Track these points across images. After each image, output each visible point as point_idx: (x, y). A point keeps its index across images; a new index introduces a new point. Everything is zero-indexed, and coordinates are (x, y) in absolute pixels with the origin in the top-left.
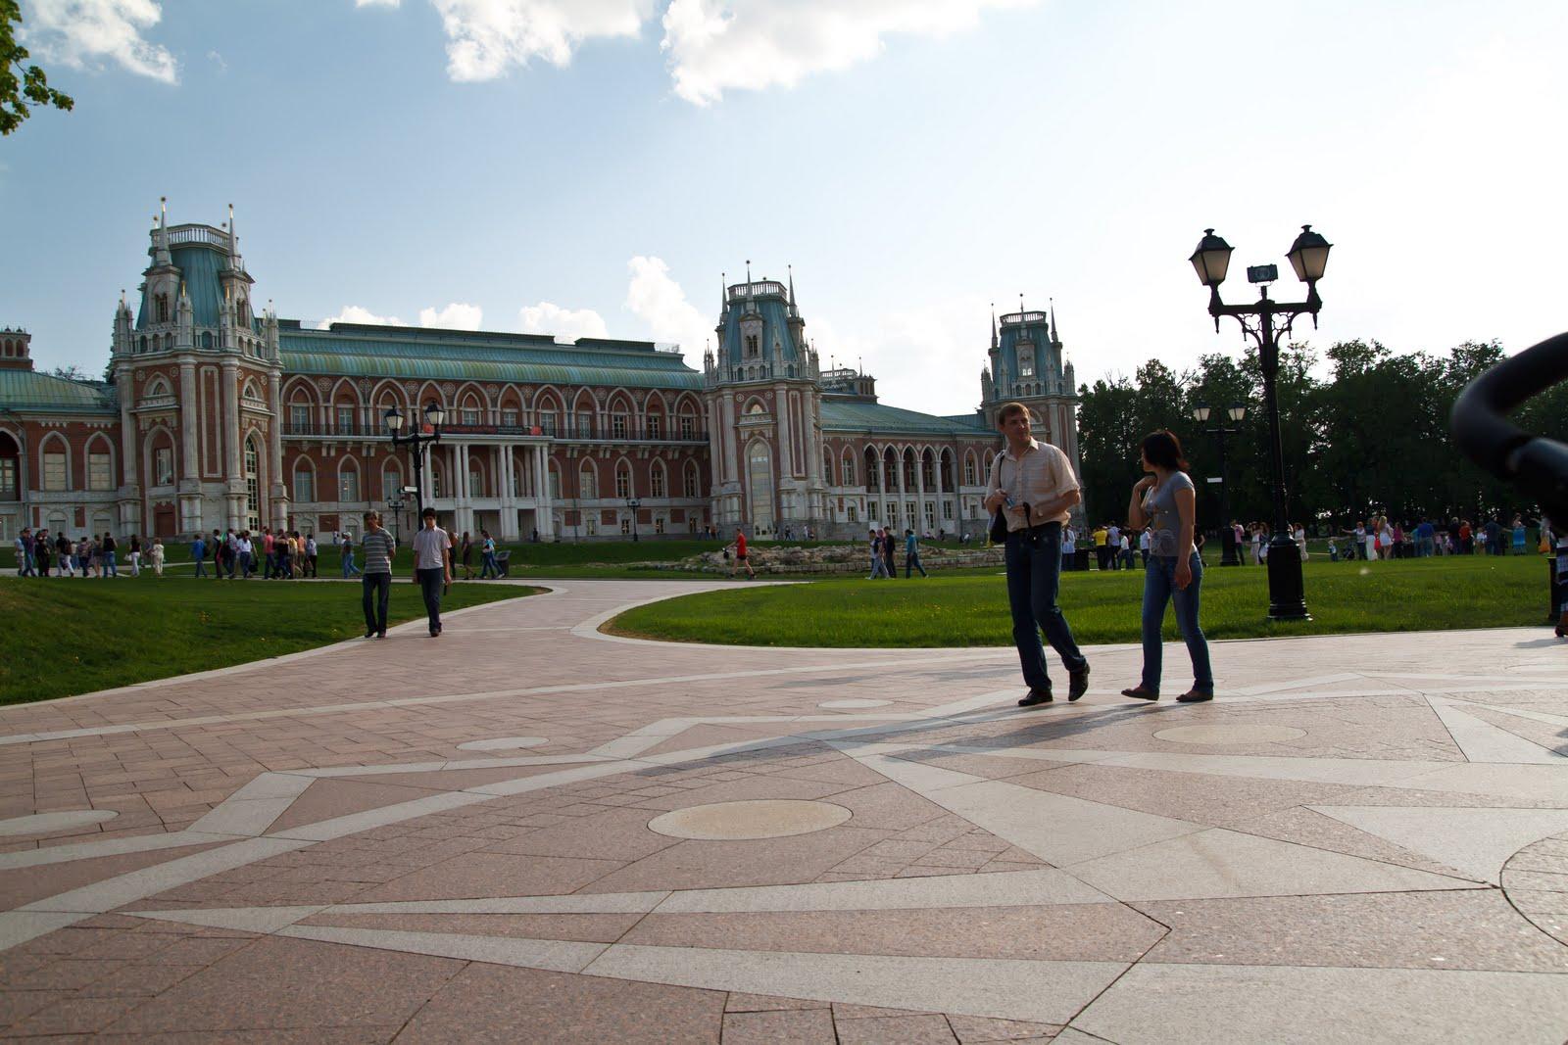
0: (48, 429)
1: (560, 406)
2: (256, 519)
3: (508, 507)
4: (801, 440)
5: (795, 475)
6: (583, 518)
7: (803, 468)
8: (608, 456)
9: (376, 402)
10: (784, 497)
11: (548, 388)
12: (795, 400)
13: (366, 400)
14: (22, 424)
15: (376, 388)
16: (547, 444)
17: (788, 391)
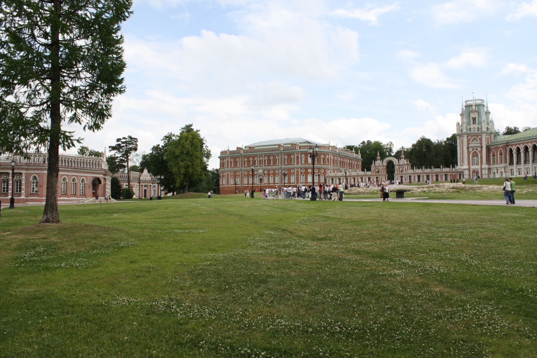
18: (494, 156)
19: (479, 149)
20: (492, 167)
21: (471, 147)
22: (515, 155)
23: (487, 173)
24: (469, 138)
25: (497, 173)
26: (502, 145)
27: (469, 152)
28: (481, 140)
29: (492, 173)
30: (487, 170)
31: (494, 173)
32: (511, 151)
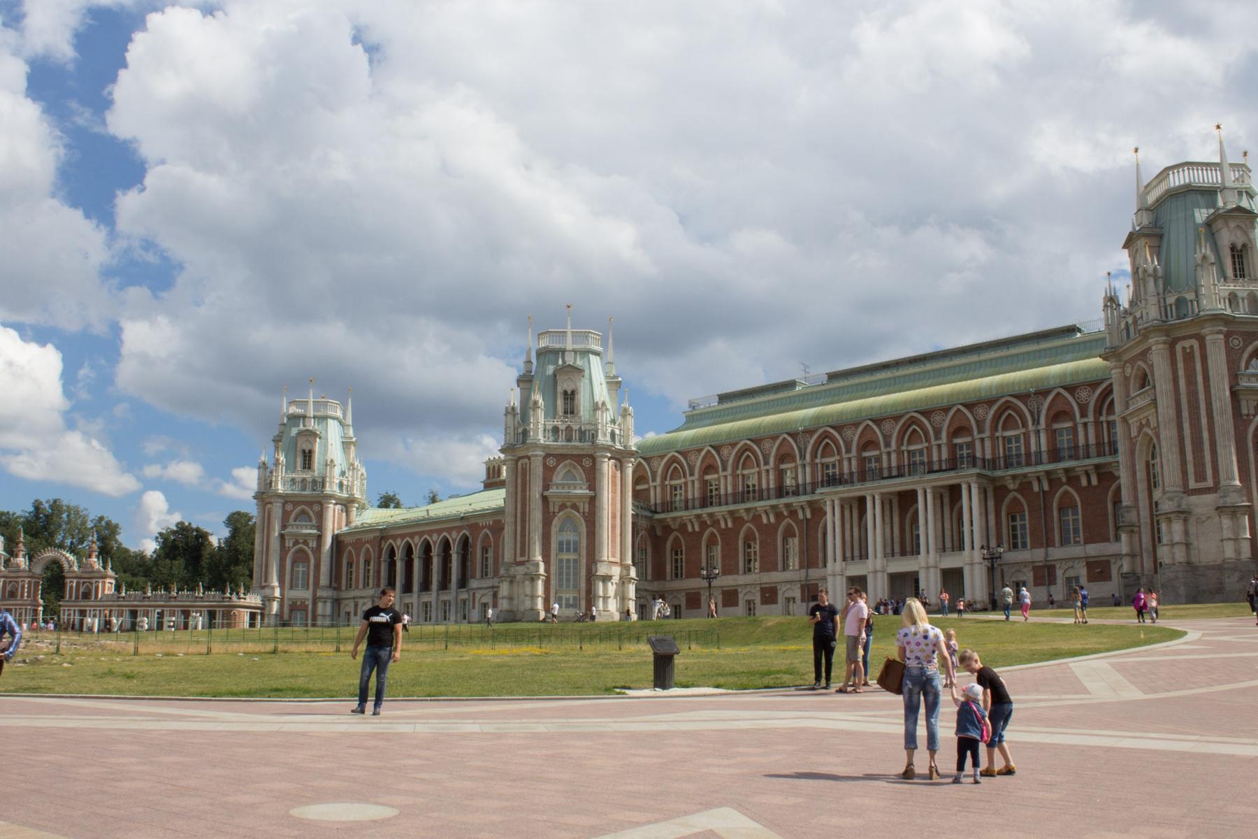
0: (483, 527)
1: (1025, 425)
2: (575, 598)
3: (927, 564)
4: (1204, 421)
5: (1192, 484)
6: (1059, 573)
7: (1209, 472)
8: (1094, 481)
9: (814, 456)
10: (1164, 526)
11: (1008, 402)
12: (1189, 357)
13: (803, 457)
14: (470, 527)
15: (812, 441)
16: (974, 478)
17: (1172, 346)
18: (350, 564)
19: (313, 544)
20: (344, 595)
21: (292, 534)
22: (399, 566)
23: (328, 612)
24: (289, 507)
25: (356, 614)
26: (371, 536)
27: (284, 550)
28: (321, 516)
29: (342, 614)
30: (329, 605)
31: (348, 614)
32: (392, 553)
